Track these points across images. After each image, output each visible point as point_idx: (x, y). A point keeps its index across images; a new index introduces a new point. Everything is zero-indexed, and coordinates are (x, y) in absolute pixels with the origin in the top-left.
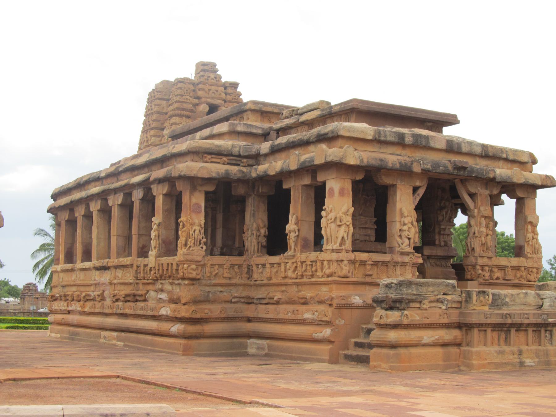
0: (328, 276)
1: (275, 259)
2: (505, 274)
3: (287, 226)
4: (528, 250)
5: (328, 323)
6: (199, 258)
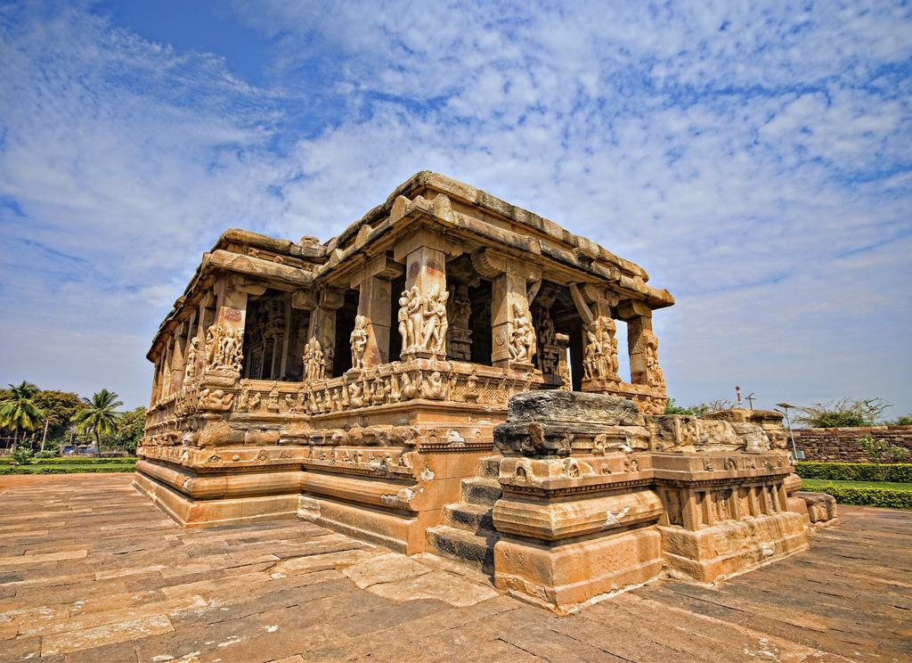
0: (409, 399)
1: (337, 381)
3: (353, 333)
4: (650, 376)
5: (407, 479)
6: (230, 381)
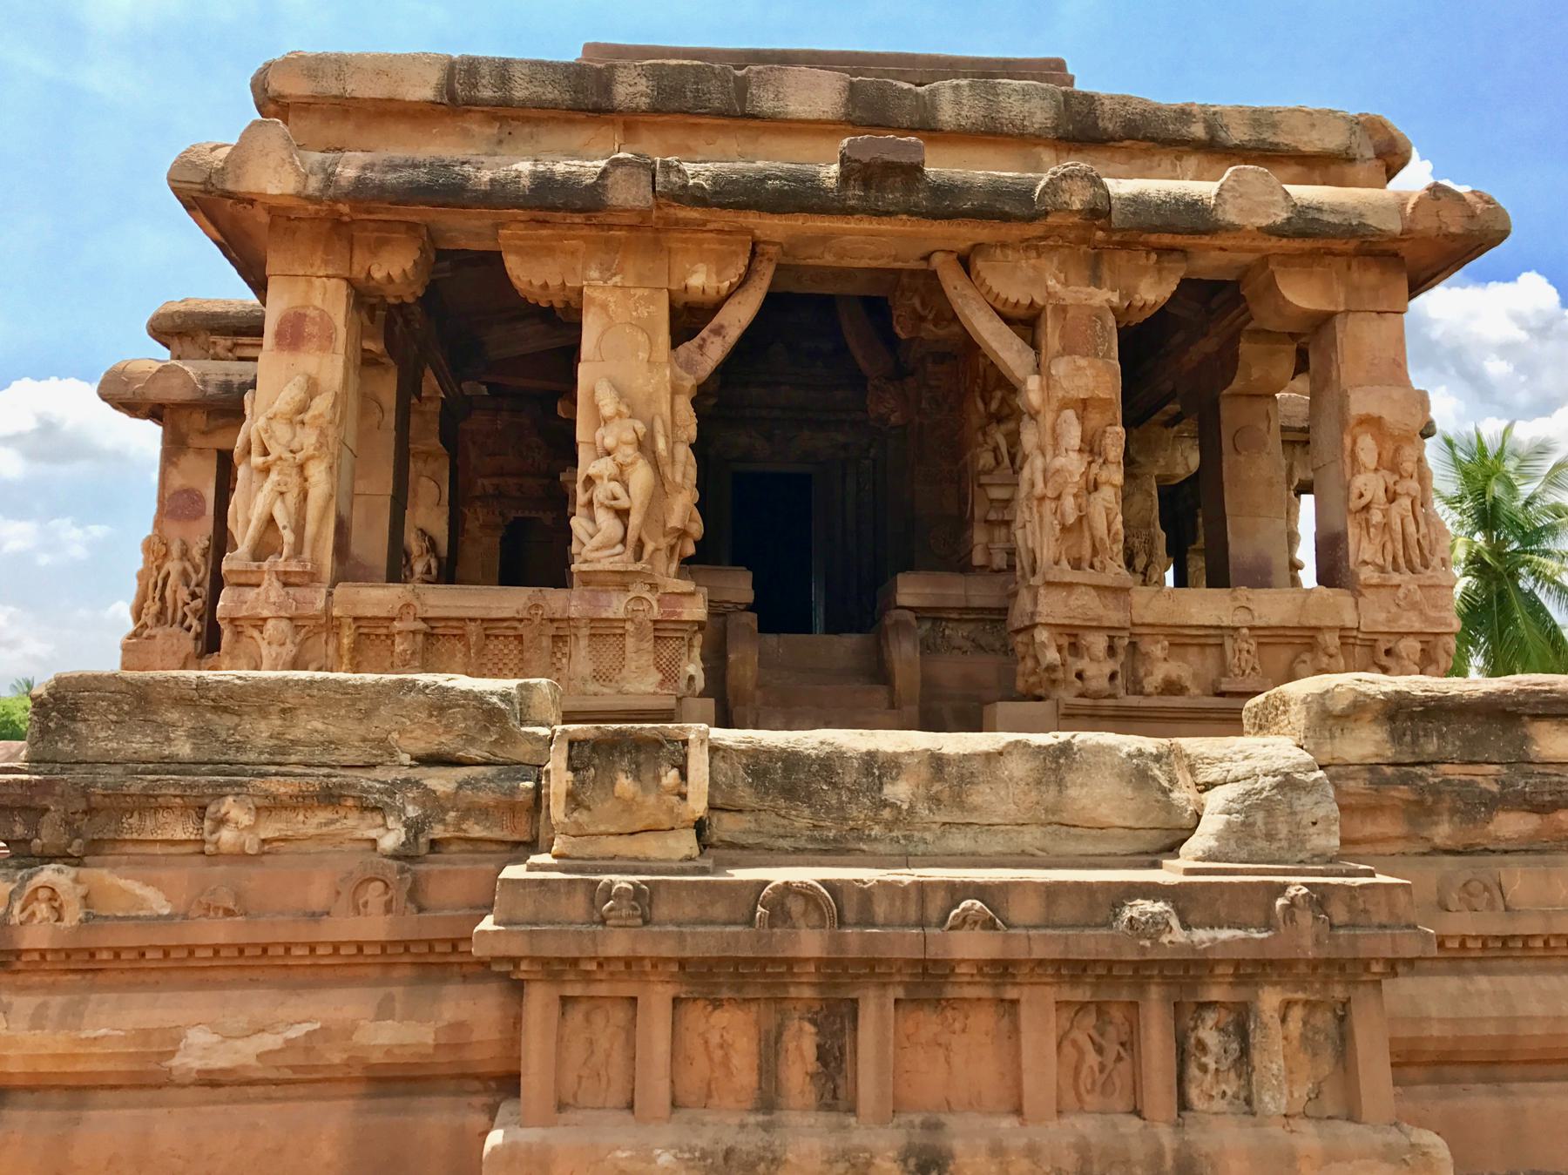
2: (1224, 671)
